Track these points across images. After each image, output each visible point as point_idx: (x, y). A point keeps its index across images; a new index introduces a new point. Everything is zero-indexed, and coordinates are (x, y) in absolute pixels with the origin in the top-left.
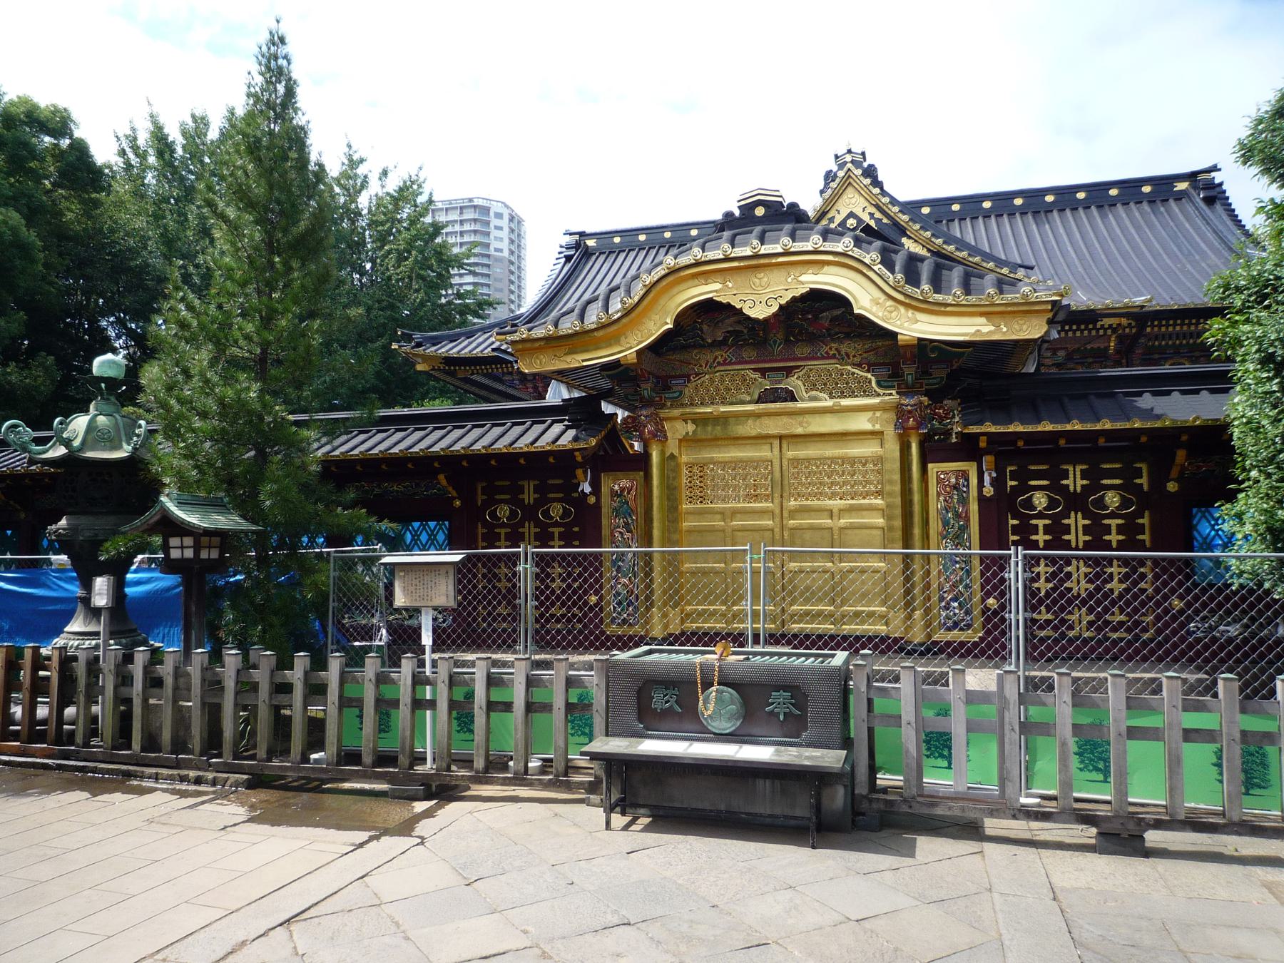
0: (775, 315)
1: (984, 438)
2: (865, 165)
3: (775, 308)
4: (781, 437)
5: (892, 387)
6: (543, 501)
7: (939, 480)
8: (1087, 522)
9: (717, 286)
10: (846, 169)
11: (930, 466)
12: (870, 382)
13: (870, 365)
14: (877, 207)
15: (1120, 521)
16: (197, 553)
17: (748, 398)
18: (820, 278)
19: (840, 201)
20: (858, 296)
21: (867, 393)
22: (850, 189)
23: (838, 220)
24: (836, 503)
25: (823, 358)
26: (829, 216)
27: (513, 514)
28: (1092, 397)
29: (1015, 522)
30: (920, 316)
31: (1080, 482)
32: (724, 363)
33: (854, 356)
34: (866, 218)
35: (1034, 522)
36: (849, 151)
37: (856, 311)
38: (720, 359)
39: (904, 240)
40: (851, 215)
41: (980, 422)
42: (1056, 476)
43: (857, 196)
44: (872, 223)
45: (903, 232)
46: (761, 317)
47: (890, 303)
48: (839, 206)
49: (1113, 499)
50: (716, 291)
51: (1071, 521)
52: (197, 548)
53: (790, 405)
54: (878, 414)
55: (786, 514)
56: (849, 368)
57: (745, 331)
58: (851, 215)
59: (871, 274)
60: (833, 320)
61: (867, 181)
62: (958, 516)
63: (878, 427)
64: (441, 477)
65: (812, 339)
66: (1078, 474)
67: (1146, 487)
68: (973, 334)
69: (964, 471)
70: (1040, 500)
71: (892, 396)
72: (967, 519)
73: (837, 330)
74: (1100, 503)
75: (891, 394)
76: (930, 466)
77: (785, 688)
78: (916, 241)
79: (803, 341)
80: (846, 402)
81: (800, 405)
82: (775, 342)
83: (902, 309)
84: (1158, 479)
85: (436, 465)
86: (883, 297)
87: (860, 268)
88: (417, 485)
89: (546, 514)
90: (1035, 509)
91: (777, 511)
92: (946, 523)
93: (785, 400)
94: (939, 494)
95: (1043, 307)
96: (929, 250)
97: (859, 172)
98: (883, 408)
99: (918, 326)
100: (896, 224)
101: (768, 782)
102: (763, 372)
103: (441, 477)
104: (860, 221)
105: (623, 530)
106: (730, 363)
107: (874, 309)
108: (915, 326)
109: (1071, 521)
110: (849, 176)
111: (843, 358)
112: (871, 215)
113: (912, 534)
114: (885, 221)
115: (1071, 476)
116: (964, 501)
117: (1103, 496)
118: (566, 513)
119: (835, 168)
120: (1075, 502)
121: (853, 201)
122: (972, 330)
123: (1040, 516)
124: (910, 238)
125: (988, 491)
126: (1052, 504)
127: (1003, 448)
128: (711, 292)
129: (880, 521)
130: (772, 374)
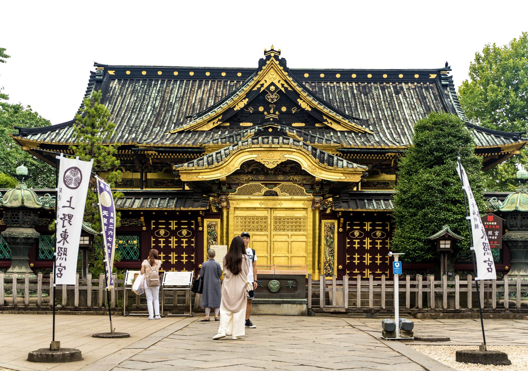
0: (275, 167)
1: (340, 213)
2: (280, 58)
3: (276, 165)
4: (271, 208)
5: (311, 193)
6: (179, 228)
7: (325, 226)
9: (256, 156)
10: (271, 60)
11: (322, 221)
12: (303, 190)
14: (285, 81)
17: (260, 194)
18: (291, 156)
19: (267, 76)
21: (303, 194)
22: (272, 70)
23: (266, 85)
24: (290, 233)
25: (287, 181)
26: (261, 83)
27: (166, 234)
29: (349, 240)
30: (323, 172)
31: (369, 228)
32: (252, 180)
33: (298, 181)
34: (280, 86)
36: (272, 50)
37: (303, 169)
38: (251, 179)
39: (299, 100)
40: (272, 84)
41: (340, 207)
42: (362, 225)
43: (275, 74)
44: (283, 89)
45: (298, 95)
46: (271, 168)
47: (314, 167)
48: (266, 78)
49: (379, 234)
50: (256, 157)
51: (366, 241)
52: (90, 241)
53: (276, 197)
54: (306, 202)
55: (272, 236)
56: (296, 185)
57: (260, 169)
58: (272, 84)
59: (308, 157)
60: (291, 168)
61: (281, 68)
62: (331, 238)
63: (306, 207)
64: (142, 218)
65: (284, 173)
66: (369, 225)
68: (339, 179)
69: (333, 223)
70: (357, 233)
71: (311, 196)
72: (334, 239)
73: (293, 171)
74: (375, 235)
75: (310, 195)
78: (304, 101)
79: (280, 174)
80: (295, 197)
81: (279, 197)
82: (271, 174)
83: (317, 169)
85: (142, 213)
87: (305, 155)
88: (126, 221)
90: (355, 236)
91: (269, 235)
92: (327, 241)
93: (274, 195)
94: (325, 231)
95: (360, 173)
96: (310, 107)
97: (277, 62)
99: (322, 175)
100: (295, 91)
101: (287, 305)
102: (266, 185)
103: (142, 218)
104: (277, 88)
105: (212, 241)
106: (255, 181)
107: (308, 168)
108: (321, 175)
110: (272, 64)
111: (295, 181)
112: (283, 85)
113: (315, 244)
114: (290, 89)
115: (367, 225)
116: (333, 233)
118: (188, 234)
119: (265, 58)
120: (368, 234)
121: (274, 76)
122: (338, 178)
124: (301, 99)
125: (341, 230)
126: (360, 235)
128: (253, 158)
130: (270, 186)
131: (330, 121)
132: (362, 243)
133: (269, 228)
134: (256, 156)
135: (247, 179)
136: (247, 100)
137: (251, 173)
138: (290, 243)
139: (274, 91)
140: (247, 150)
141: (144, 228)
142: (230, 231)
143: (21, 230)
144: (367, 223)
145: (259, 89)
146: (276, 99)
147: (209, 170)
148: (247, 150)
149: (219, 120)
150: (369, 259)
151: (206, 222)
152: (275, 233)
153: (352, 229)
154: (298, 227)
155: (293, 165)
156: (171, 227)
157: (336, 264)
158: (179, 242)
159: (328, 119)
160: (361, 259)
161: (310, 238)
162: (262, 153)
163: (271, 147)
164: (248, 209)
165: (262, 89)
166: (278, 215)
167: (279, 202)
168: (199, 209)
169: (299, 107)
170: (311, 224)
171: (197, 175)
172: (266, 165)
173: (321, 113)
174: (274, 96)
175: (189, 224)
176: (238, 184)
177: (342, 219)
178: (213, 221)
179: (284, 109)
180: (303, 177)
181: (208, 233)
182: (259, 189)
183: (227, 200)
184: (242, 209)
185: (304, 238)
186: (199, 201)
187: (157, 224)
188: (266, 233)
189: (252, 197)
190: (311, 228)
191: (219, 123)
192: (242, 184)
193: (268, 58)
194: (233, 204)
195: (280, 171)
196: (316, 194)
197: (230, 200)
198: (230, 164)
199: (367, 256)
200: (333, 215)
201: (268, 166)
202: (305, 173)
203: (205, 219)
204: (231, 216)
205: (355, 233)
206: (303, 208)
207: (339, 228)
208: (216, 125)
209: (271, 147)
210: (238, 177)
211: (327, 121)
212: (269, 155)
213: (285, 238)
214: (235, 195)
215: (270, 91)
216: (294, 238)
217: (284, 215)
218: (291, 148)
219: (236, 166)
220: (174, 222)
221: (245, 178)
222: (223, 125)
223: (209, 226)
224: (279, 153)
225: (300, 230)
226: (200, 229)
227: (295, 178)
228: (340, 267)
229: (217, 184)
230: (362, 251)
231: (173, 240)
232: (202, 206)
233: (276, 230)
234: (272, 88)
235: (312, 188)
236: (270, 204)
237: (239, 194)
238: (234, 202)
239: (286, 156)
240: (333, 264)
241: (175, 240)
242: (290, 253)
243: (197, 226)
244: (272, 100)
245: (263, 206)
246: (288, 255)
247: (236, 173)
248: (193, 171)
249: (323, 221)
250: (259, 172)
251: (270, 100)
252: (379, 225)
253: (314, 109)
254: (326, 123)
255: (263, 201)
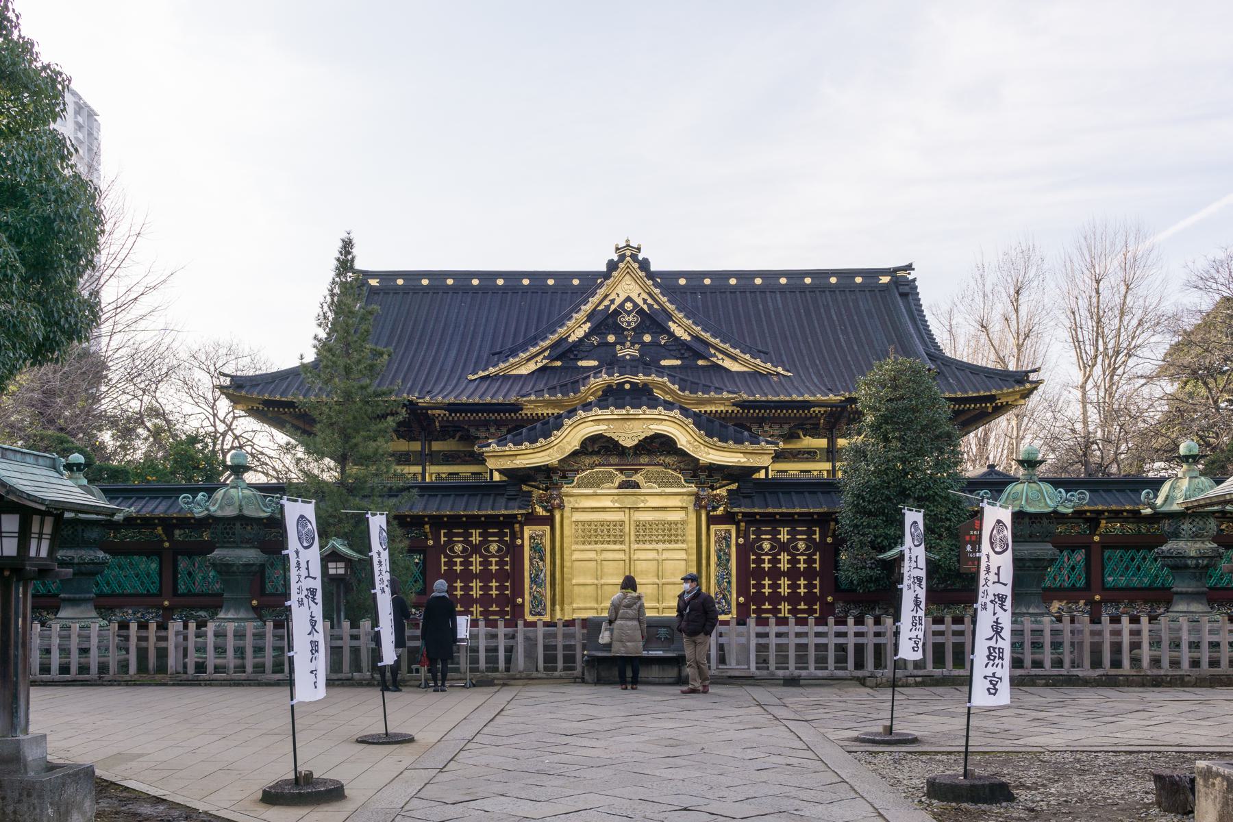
0: (636, 445)
2: (640, 258)
3: (636, 442)
4: (630, 508)
6: (485, 542)
7: (716, 534)
8: (789, 557)
9: (605, 427)
10: (625, 261)
11: (711, 526)
13: (681, 470)
14: (650, 294)
15: (805, 557)
16: (346, 571)
19: (619, 286)
20: (679, 437)
21: (679, 485)
23: (618, 302)
24: (660, 546)
25: (655, 465)
26: (610, 298)
27: (464, 550)
28: (793, 493)
29: (754, 557)
30: (711, 451)
31: (786, 537)
32: (600, 465)
34: (640, 302)
35: (763, 557)
36: (628, 246)
37: (679, 447)
38: (597, 462)
39: (670, 324)
40: (629, 299)
41: (739, 506)
43: (633, 283)
44: (645, 307)
45: (670, 317)
46: (629, 446)
47: (696, 443)
48: (619, 290)
49: (802, 546)
51: (781, 557)
52: (346, 568)
53: (637, 490)
54: (685, 497)
55: (632, 552)
58: (629, 299)
59: (687, 429)
61: (642, 274)
62: (725, 554)
63: (684, 505)
64: (427, 527)
65: (650, 453)
67: (818, 540)
70: (766, 546)
71: (693, 489)
72: (730, 555)
73: (663, 449)
74: (796, 548)
76: (711, 526)
77: (664, 627)
80: (668, 490)
81: (642, 491)
82: (629, 454)
83: (702, 446)
84: (823, 536)
85: (426, 519)
86: (693, 440)
87: (683, 426)
89: (487, 550)
90: (764, 550)
91: (627, 550)
92: (719, 558)
93: (633, 487)
94: (716, 542)
96: (689, 334)
98: (689, 494)
99: (710, 456)
100: (664, 310)
102: (621, 471)
103: (427, 527)
104: (635, 305)
105: (538, 560)
106: (603, 465)
109: (781, 557)
111: (667, 466)
112: (645, 301)
114: (656, 306)
116: (729, 546)
117: (797, 544)
118: (500, 550)
119: (616, 259)
120: (784, 547)
121: (631, 287)
122: (736, 460)
123: (767, 554)
124: (675, 322)
125: (741, 541)
126: (773, 548)
127: (750, 519)
129: (684, 556)
131: (720, 356)
132: (775, 561)
133: (627, 539)
134: (605, 427)
135: (592, 462)
136: (589, 324)
137: (597, 453)
138: (660, 562)
139: (631, 311)
140: (590, 419)
141: (431, 542)
142: (565, 545)
143: (239, 552)
144: (782, 529)
145: (608, 307)
146: (635, 322)
147: (531, 451)
148: (590, 419)
149: (545, 358)
150: (786, 586)
151: (528, 531)
152: (636, 546)
153: (758, 539)
154: (673, 538)
155: (663, 440)
156: (473, 539)
157: (734, 596)
158: (485, 563)
159: (717, 354)
160: (775, 586)
161: (692, 554)
162: (615, 422)
163: (628, 414)
164: (594, 509)
165: (613, 307)
166: (641, 519)
167: (642, 498)
168: (527, 596)
169: (671, 335)
170: (694, 532)
171: (512, 458)
172: (620, 442)
173: (707, 344)
174: (631, 319)
175: (501, 535)
176: (577, 471)
177: (743, 524)
178: (538, 529)
179: (647, 338)
180: (680, 459)
181: (531, 548)
182: (611, 478)
183: (560, 496)
184: (584, 510)
185: (683, 555)
186: (515, 499)
187: (449, 535)
188: (623, 547)
189: (599, 491)
190: (694, 538)
191: (545, 362)
192: (583, 470)
193: (622, 258)
194: (569, 503)
195: (643, 449)
196: (700, 485)
197: (566, 496)
198: (564, 441)
199: (784, 582)
200: (729, 518)
201: (624, 444)
202: (683, 454)
203: (525, 527)
204: (566, 522)
205: (764, 545)
206: (681, 508)
207: (738, 537)
208: (540, 365)
209: (628, 414)
210: (577, 459)
211: (717, 357)
212: (627, 426)
213: (652, 555)
214: (573, 487)
215: (626, 311)
216: (666, 555)
217: (650, 519)
218: (660, 414)
219: (573, 445)
220: (478, 531)
221: (588, 460)
222: (550, 365)
223: (531, 537)
224: (641, 421)
225: (676, 542)
226: (519, 542)
227: (668, 460)
228: (742, 599)
229: (543, 471)
230: (775, 574)
231: (476, 559)
232: (520, 508)
233: (638, 542)
234: (629, 306)
235: (694, 476)
236: (629, 502)
237: (579, 487)
238: (571, 499)
239: (651, 427)
240: (730, 595)
241: (479, 560)
242: (660, 579)
243: (514, 536)
244: (629, 324)
245: (617, 505)
246: (657, 581)
247: (575, 454)
248: (507, 453)
249: (713, 528)
250: (611, 451)
251: (624, 325)
252: (801, 533)
253: (696, 338)
254: (714, 359)
255: (616, 498)
